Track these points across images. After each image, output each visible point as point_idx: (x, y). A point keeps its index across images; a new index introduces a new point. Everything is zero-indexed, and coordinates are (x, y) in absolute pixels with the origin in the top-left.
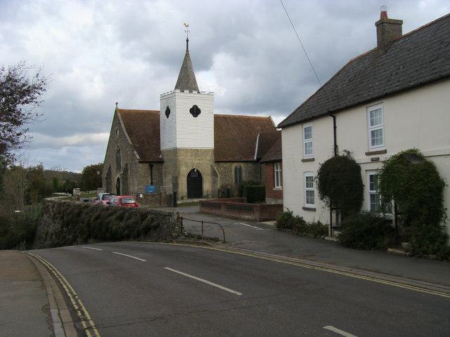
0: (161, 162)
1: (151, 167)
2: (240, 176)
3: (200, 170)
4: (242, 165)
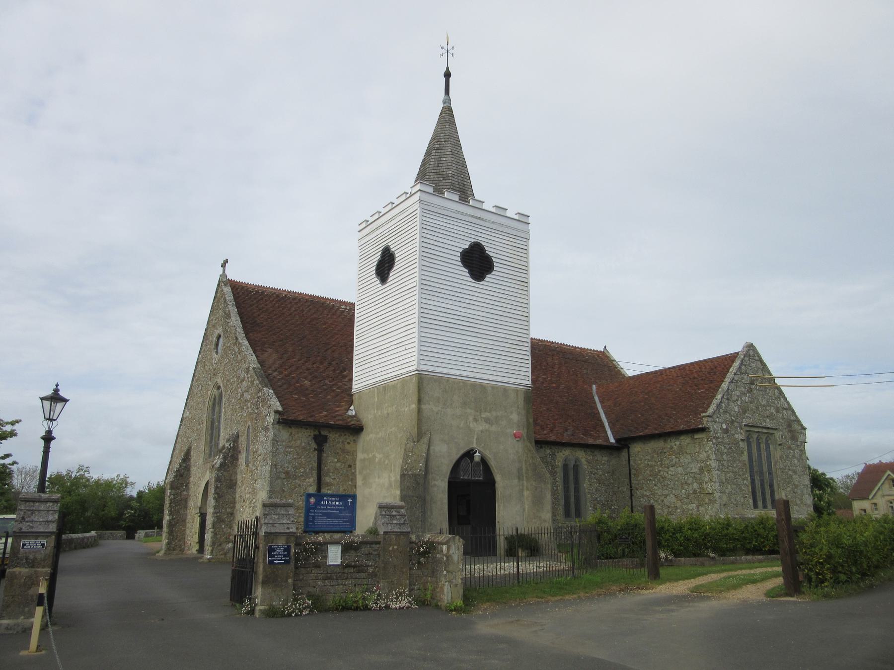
0: (356, 429)
1: (320, 441)
2: (577, 490)
3: (493, 464)
4: (581, 454)
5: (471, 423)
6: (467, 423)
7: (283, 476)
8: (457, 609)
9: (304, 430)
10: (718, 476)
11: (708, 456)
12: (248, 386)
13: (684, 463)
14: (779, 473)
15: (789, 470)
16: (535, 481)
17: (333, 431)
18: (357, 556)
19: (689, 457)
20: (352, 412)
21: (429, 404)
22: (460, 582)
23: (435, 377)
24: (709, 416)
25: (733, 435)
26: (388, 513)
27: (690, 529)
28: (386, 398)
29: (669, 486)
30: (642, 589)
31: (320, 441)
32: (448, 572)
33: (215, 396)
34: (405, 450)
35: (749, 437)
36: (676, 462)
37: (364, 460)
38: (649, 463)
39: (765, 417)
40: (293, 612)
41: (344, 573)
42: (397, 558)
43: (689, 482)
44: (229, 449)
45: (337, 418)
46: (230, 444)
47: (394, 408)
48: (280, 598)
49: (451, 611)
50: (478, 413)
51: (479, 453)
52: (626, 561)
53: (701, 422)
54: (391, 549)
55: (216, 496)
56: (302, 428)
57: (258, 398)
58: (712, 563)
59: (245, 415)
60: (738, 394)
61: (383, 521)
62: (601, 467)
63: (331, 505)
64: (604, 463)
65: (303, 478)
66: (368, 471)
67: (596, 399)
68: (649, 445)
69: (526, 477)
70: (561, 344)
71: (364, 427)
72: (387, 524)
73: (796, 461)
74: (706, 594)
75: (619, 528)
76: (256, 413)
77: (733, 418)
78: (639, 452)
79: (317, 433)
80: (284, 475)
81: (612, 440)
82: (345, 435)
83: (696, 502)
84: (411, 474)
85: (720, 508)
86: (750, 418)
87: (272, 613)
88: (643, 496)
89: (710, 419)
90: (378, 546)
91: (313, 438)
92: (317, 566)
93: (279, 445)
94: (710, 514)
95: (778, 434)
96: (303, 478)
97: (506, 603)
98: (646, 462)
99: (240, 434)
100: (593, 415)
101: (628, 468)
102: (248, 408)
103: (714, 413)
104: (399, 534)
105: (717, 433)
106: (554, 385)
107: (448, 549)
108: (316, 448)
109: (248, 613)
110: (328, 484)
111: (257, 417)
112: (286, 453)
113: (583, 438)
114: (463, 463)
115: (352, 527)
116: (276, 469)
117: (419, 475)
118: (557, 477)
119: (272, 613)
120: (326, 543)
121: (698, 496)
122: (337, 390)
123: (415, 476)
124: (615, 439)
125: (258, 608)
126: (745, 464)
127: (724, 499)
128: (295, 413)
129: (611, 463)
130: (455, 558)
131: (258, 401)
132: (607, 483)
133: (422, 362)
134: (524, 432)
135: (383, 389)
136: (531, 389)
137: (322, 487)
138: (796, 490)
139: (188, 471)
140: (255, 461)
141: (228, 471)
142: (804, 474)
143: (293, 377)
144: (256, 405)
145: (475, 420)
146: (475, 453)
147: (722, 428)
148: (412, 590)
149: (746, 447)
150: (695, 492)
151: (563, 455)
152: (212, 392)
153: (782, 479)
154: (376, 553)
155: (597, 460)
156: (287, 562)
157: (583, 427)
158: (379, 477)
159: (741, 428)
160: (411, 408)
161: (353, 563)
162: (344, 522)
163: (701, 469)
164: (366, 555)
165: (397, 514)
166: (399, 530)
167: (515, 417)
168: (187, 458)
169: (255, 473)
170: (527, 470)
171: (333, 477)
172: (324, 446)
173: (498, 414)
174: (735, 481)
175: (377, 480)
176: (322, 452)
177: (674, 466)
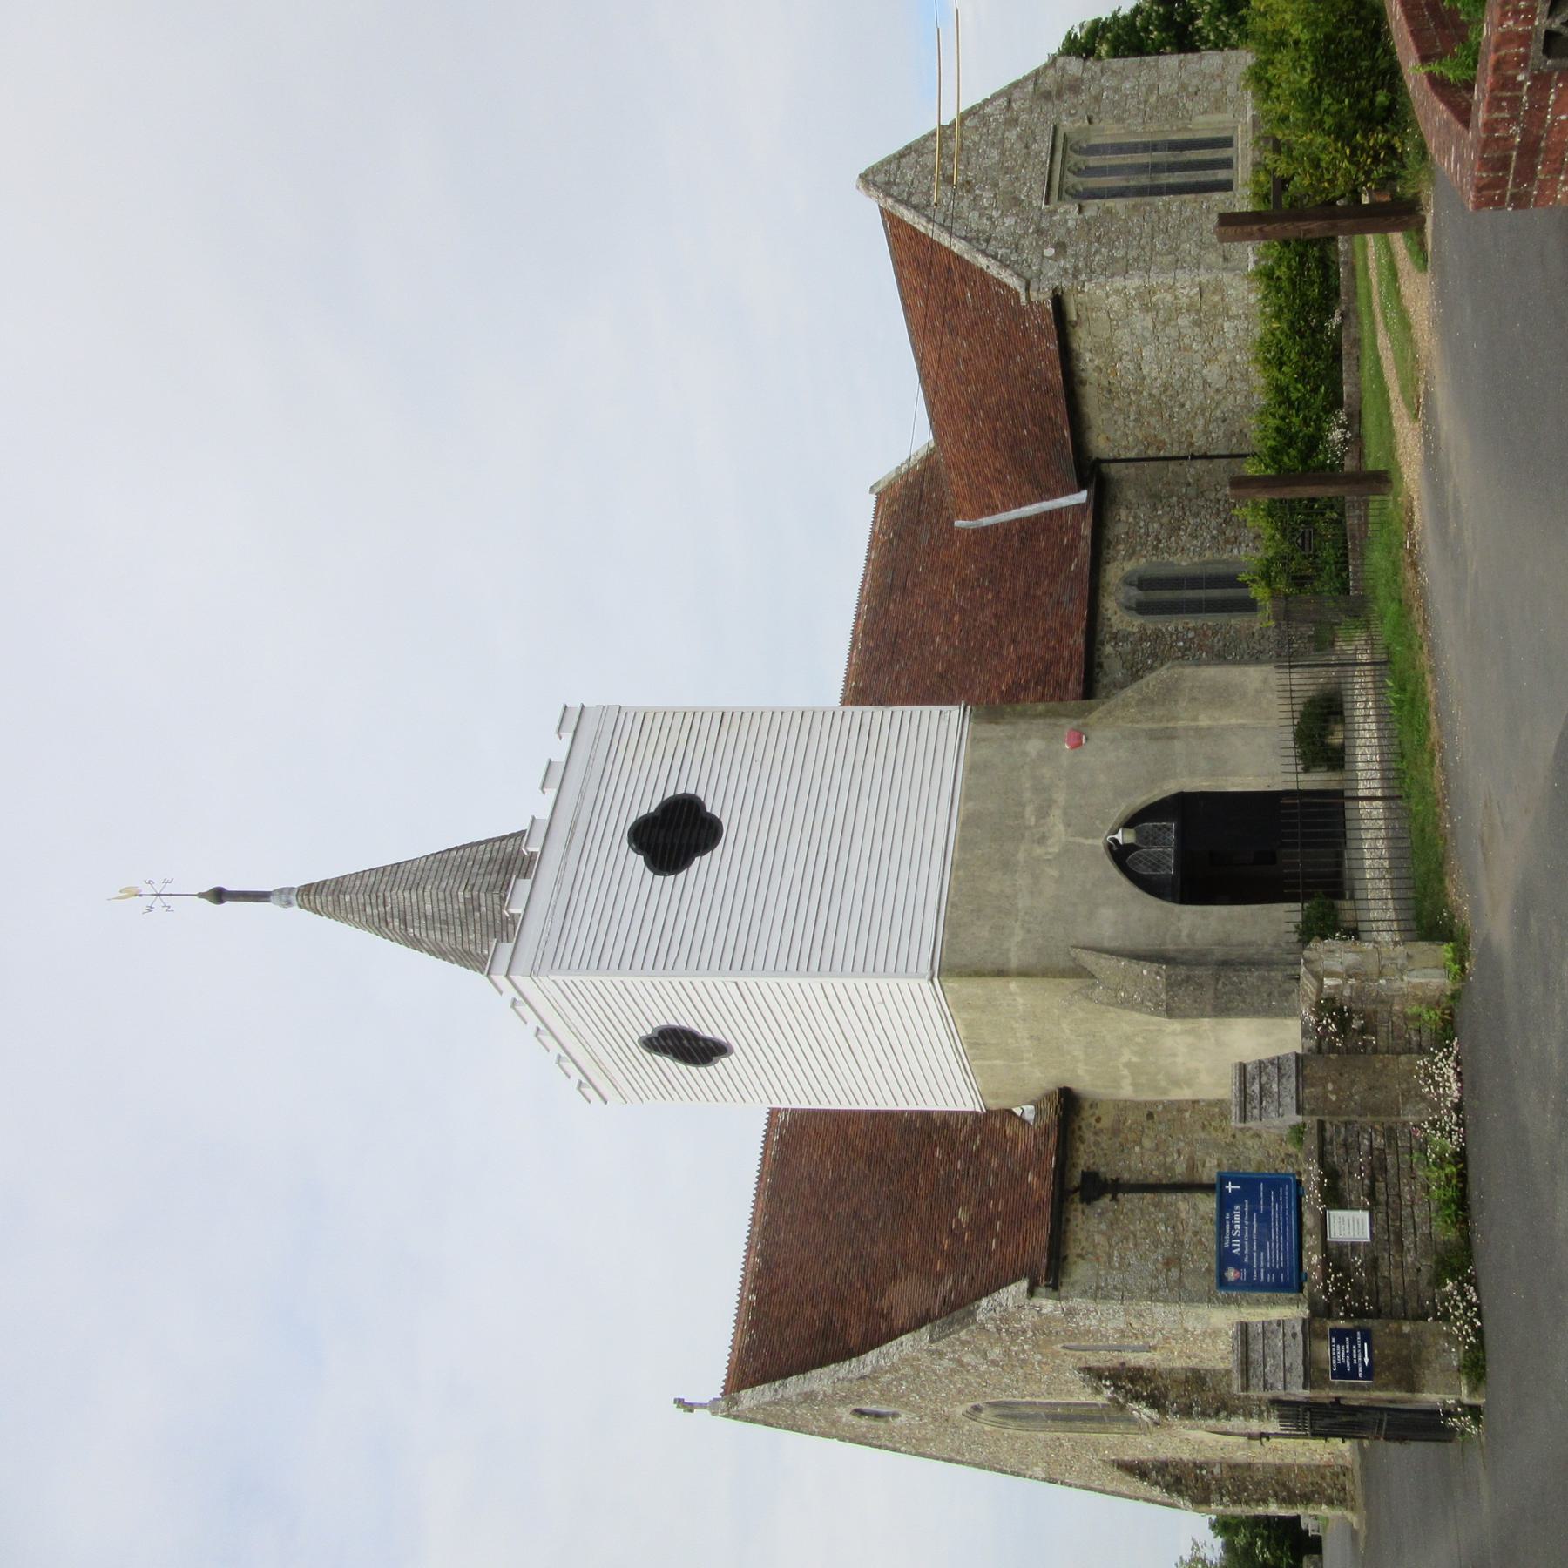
0: (1068, 1103)
1: (1096, 1187)
2: (1194, 582)
3: (1141, 800)
4: (1117, 571)
5: (1051, 850)
6: (1048, 860)
7: (1174, 1272)
8: (1461, 957)
9: (1073, 1223)
10: (1162, 271)
11: (1117, 291)
12: (972, 1352)
13: (1132, 343)
14: (1152, 127)
15: (1146, 102)
16: (1176, 702)
17: (1072, 1158)
18: (1351, 1173)
19: (1118, 333)
20: (1029, 1112)
21: (1008, 950)
22: (1402, 948)
23: (946, 937)
24: (1027, 289)
25: (1069, 232)
26: (1256, 1102)
27: (1281, 365)
28: (993, 1042)
29: (1185, 376)
30: (1412, 521)
31: (1096, 1187)
32: (1381, 975)
33: (995, 1416)
34: (1112, 1005)
35: (1073, 191)
36: (1130, 361)
37: (1135, 1085)
38: (1132, 417)
39: (1029, 154)
40: (1472, 1324)
41: (1387, 1203)
42: (1353, 1083)
43: (1174, 333)
44: (1117, 1388)
45: (1042, 1148)
46: (1105, 1386)
47: (1018, 1025)
48: (1444, 1351)
49: (1463, 969)
50: (1027, 834)
51: (1116, 832)
52: (1351, 521)
53: (1041, 305)
54: (1334, 1098)
55: (1223, 1414)
56: (1065, 1232)
57: (999, 1331)
58: (1354, 320)
59: (1039, 1357)
60: (974, 215)
61: (1273, 1115)
62: (1142, 524)
63: (1242, 1230)
64: (1135, 517)
65: (1179, 1225)
66: (1159, 1077)
67: (987, 521)
68: (1091, 416)
69: (1168, 721)
70: (861, 595)
71: (1062, 1086)
72: (1280, 1105)
73: (1128, 85)
74: (1422, 395)
75: (1278, 536)
76: (1034, 1335)
77: (1031, 231)
78: (1108, 438)
79: (1077, 1197)
80: (1173, 1270)
81: (1082, 497)
82: (1080, 1128)
83: (1220, 321)
84: (1167, 993)
85: (1233, 270)
86: (1031, 188)
87: (1476, 1368)
88: (1206, 432)
89: (1034, 285)
90: (1328, 1126)
91: (1089, 1203)
92: (1373, 1265)
93: (1107, 1285)
94: (1246, 293)
95: (1067, 125)
96: (1179, 1225)
97: (1446, 839)
98: (1131, 424)
99: (1083, 1365)
100: (1023, 534)
101: (1145, 464)
102: (1024, 1351)
103: (1019, 275)
104: (1301, 1079)
105: (1066, 270)
106: (957, 618)
107: (1332, 975)
108: (1110, 1196)
109: (1476, 1420)
110: (1192, 1167)
111: (1043, 1332)
112: (1124, 1266)
113: (1077, 565)
114: (1145, 871)
115: (1288, 1181)
116: (1158, 1288)
117: (1168, 978)
118: (1167, 629)
119: (1476, 1368)
120: (1325, 1246)
121: (1205, 316)
122: (978, 1142)
123: (1170, 986)
124: (1079, 491)
125: (1466, 1400)
126: (1134, 206)
127: (1214, 259)
128: (1033, 1248)
129: (1134, 501)
130: (1350, 958)
131: (1007, 1331)
132: (1177, 512)
133: (912, 968)
134: (1068, 724)
135: (974, 1047)
136: (969, 707)
137: (1197, 1181)
138: (1190, 89)
139: (1167, 1466)
140: (1143, 1334)
141: (1166, 1387)
142: (1156, 66)
143: (949, 1246)
144: (1014, 1335)
145: (1042, 840)
146: (1115, 841)
147: (1054, 258)
148: (1420, 1045)
149: (1097, 201)
150: (1198, 323)
151: (1116, 613)
152: (987, 1424)
153: (1166, 119)
154: (1343, 1130)
155: (1127, 533)
156: (1367, 1336)
157: (1052, 561)
158: (1175, 1055)
159: (1055, 212)
160: (1018, 990)
161: (1366, 1182)
162: (1277, 1200)
163: (1146, 308)
164: (1347, 1153)
165: (1257, 1081)
166: (1293, 1079)
167: (1034, 746)
168: (1138, 1470)
169: (1170, 1332)
170: (1152, 718)
171: (1176, 1156)
172: (1106, 1179)
173: (1028, 785)
174: (1172, 231)
175: (1180, 1060)
176: (1121, 1181)
177: (1140, 365)
